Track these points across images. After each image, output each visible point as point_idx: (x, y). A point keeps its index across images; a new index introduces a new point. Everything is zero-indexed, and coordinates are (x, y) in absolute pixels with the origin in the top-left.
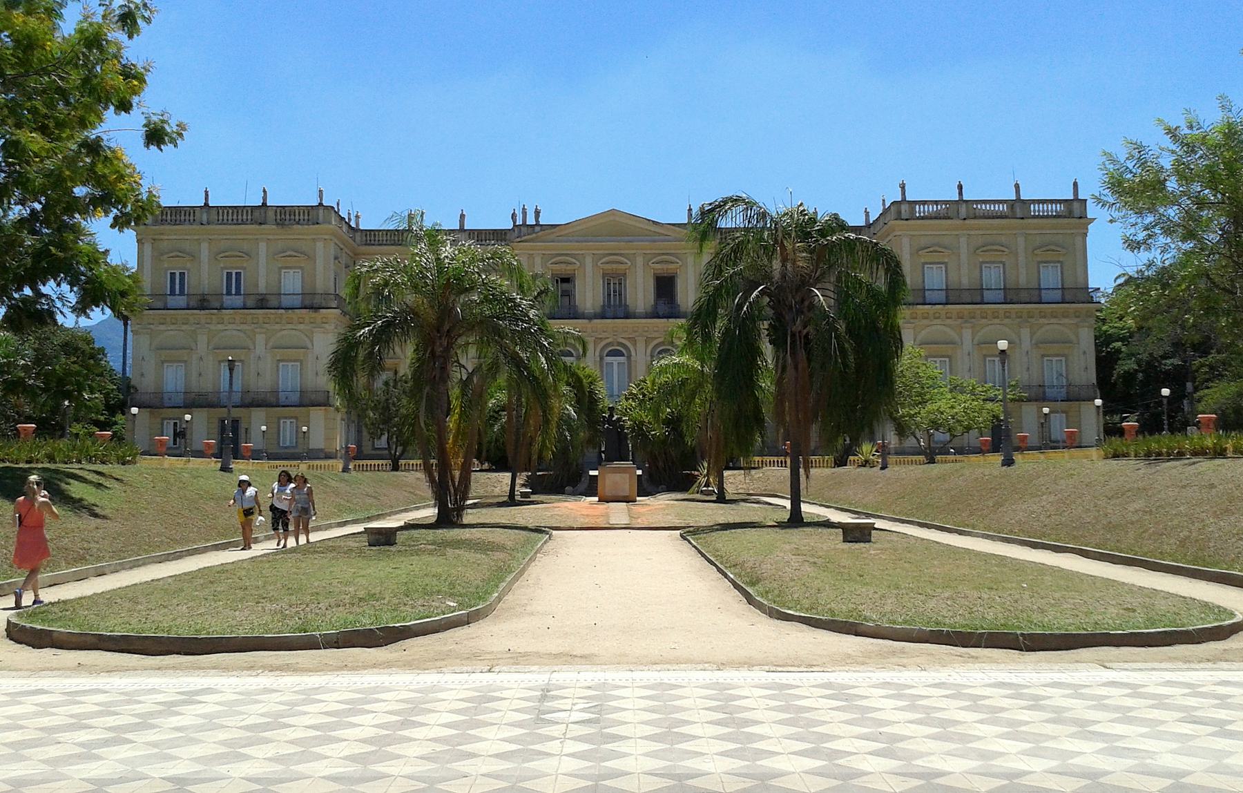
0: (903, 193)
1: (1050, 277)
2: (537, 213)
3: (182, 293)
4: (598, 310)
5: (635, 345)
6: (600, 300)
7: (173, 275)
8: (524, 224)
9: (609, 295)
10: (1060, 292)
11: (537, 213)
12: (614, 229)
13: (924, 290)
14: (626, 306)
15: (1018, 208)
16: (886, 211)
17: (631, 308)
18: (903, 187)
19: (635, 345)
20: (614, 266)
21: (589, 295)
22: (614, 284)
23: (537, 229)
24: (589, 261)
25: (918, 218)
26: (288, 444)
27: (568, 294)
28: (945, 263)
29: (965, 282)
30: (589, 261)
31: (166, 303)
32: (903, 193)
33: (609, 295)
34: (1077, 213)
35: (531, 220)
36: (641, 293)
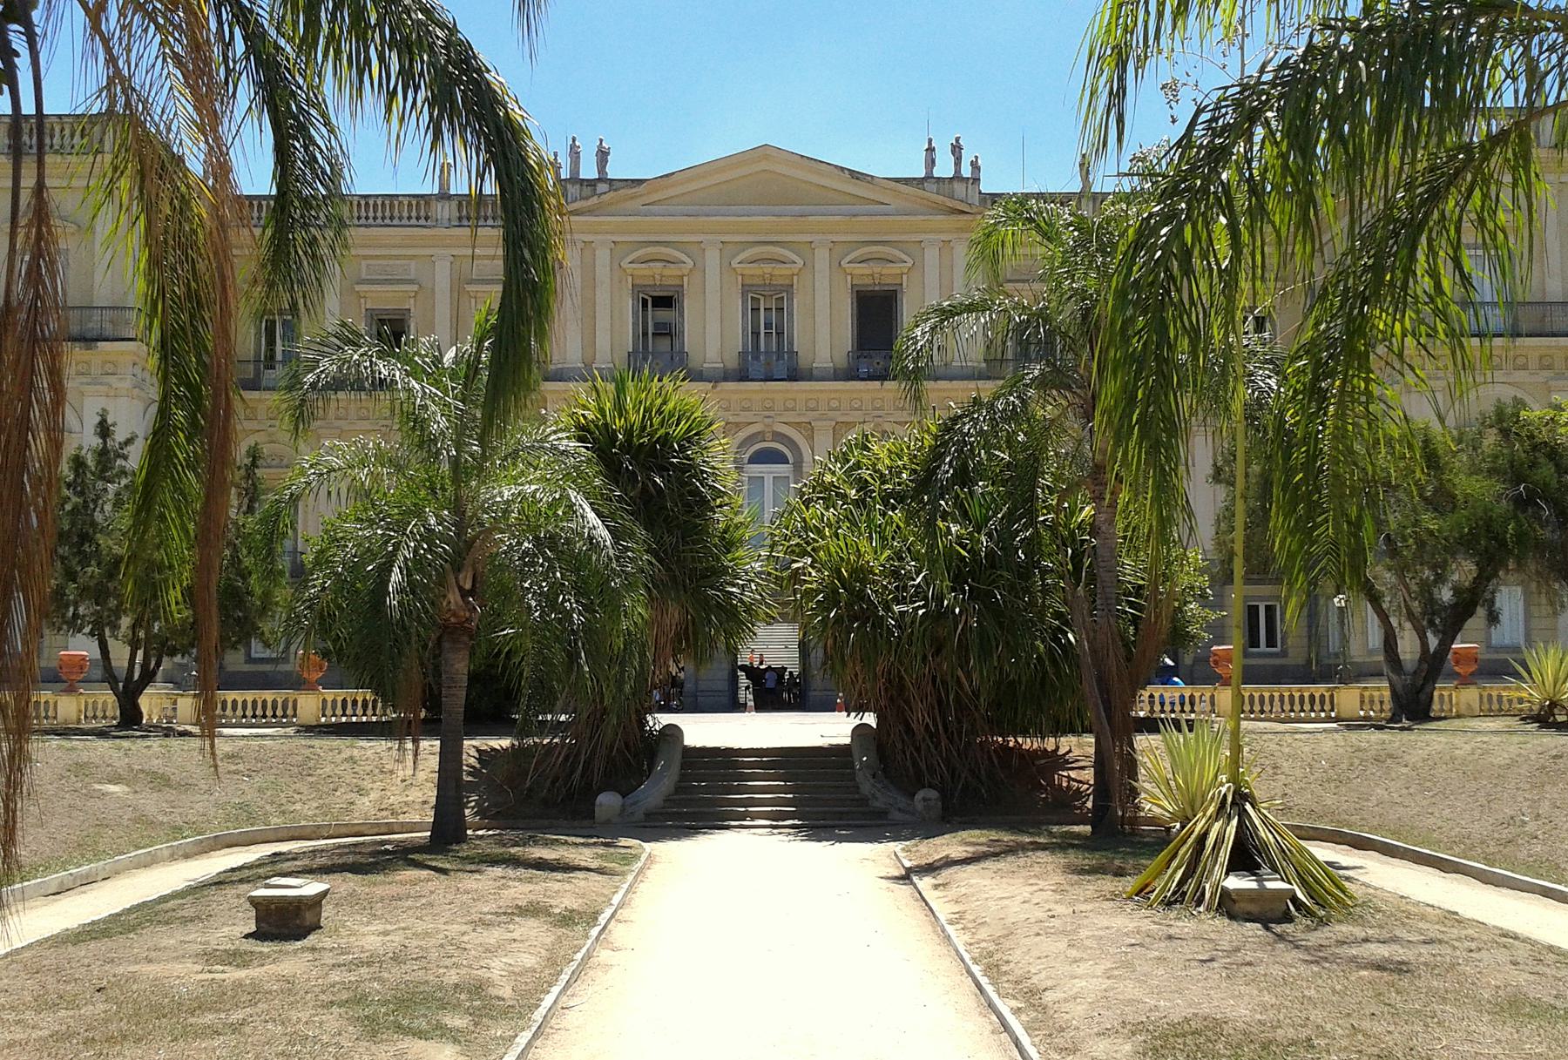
2: (603, 155)
4: (732, 363)
5: (810, 438)
6: (737, 341)
8: (575, 179)
9: (756, 334)
11: (603, 155)
12: (770, 185)
14: (792, 353)
17: (803, 362)
19: (810, 438)
20: (767, 268)
21: (713, 328)
22: (768, 310)
23: (602, 187)
24: (712, 259)
27: (667, 332)
30: (712, 259)
33: (756, 334)
35: (589, 171)
36: (825, 329)
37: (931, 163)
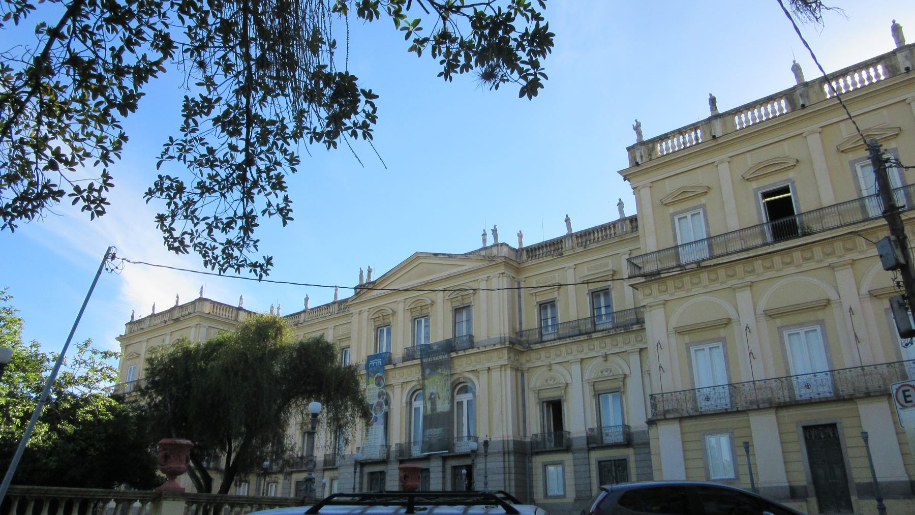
0: (639, 134)
28: (703, 206)
37: (484, 241)
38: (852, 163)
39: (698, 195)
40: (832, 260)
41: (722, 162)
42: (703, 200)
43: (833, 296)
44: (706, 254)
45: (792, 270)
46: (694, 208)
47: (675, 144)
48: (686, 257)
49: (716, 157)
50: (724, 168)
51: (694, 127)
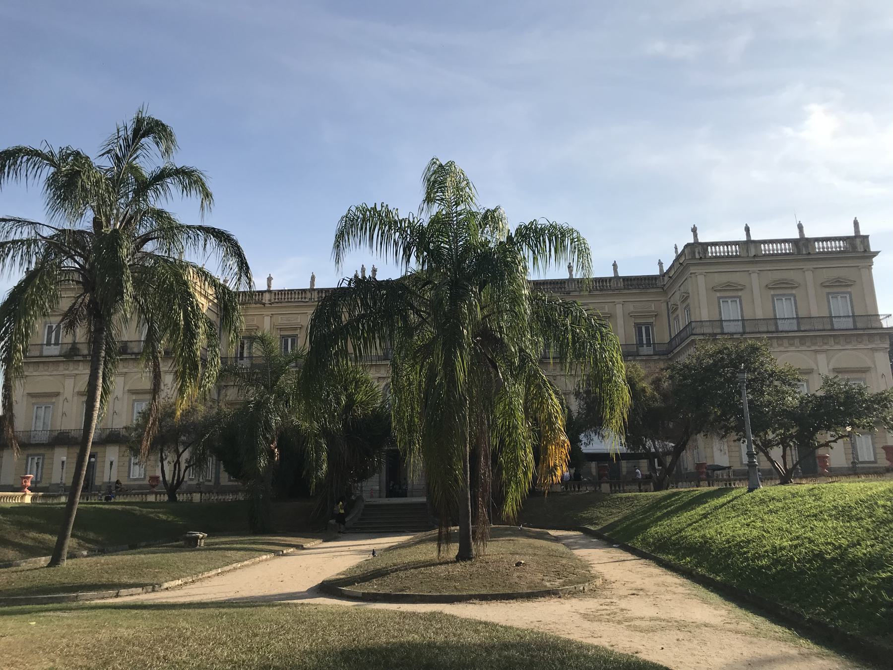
0: (695, 235)
1: (840, 307)
2: (374, 271)
3: (57, 344)
7: (50, 327)
10: (851, 320)
11: (374, 271)
13: (721, 321)
15: (802, 246)
16: (678, 257)
18: (694, 230)
25: (710, 258)
26: (137, 477)
28: (740, 297)
29: (759, 315)
31: (41, 351)
32: (695, 235)
34: (860, 248)
38: (828, 294)
39: (737, 290)
40: (817, 348)
41: (754, 272)
42: (740, 294)
43: (815, 368)
44: (741, 330)
45: (793, 348)
46: (734, 297)
47: (721, 250)
48: (729, 328)
49: (751, 268)
50: (754, 276)
51: (736, 243)
